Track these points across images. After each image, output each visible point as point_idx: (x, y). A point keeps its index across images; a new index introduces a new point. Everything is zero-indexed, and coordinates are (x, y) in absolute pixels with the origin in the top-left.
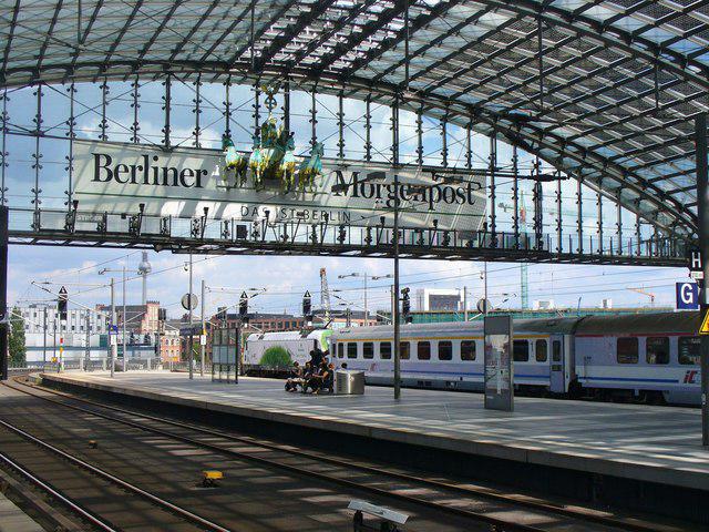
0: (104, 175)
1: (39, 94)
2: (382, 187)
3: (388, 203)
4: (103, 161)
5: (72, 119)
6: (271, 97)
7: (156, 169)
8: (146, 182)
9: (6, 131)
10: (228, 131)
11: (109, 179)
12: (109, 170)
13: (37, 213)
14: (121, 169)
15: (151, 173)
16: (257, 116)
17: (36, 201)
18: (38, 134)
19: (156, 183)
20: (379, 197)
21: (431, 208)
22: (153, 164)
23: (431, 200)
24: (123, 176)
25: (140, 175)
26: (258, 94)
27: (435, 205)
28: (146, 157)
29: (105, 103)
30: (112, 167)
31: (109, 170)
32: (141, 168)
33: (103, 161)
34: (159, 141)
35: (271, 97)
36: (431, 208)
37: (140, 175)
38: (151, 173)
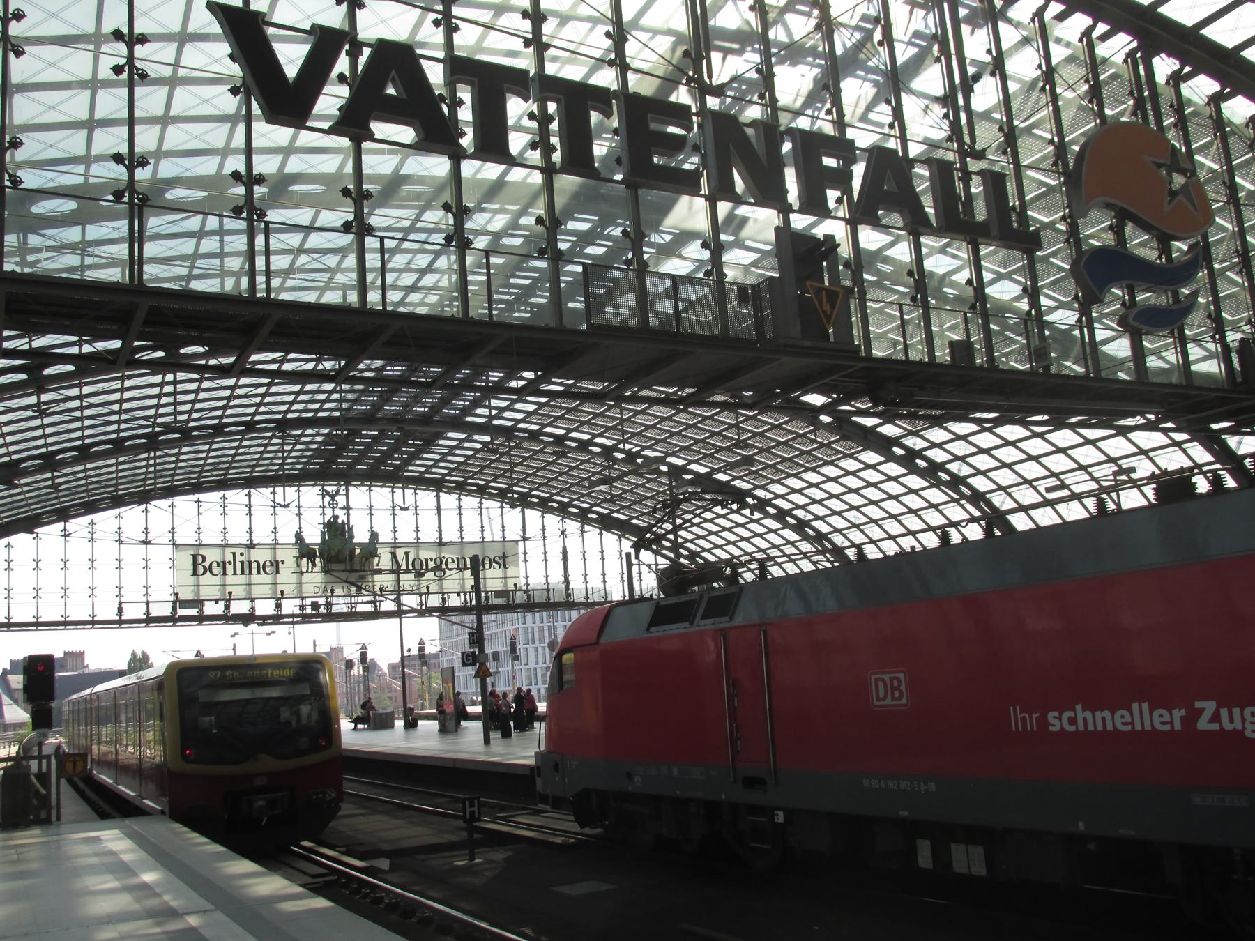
1: (146, 511)
4: (200, 559)
5: (173, 529)
6: (333, 500)
7: (242, 563)
8: (235, 573)
9: (121, 543)
10: (300, 528)
11: (205, 572)
12: (204, 567)
13: (148, 603)
14: (215, 564)
15: (239, 566)
16: (324, 514)
17: (147, 594)
18: (146, 542)
19: (243, 573)
22: (239, 558)
24: (215, 570)
25: (229, 568)
26: (323, 497)
28: (234, 554)
29: (199, 514)
30: (207, 564)
31: (204, 567)
32: (230, 563)
33: (200, 559)
34: (244, 540)
35: (333, 500)
38: (239, 566)
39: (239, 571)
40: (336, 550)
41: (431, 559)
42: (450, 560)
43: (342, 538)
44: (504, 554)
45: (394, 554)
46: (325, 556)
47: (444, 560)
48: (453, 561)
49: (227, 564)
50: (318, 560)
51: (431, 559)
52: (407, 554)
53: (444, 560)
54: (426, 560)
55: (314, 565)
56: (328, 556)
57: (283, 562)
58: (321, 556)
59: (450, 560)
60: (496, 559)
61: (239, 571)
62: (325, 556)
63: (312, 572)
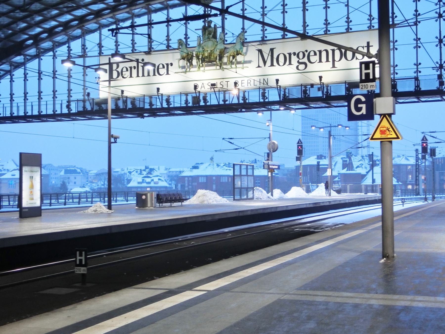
0: (115, 74)
2: (292, 56)
3: (297, 68)
12: (118, 72)
20: (290, 64)
21: (334, 66)
23: (334, 60)
25: (134, 72)
27: (336, 64)
30: (119, 70)
31: (118, 72)
32: (135, 68)
36: (334, 66)
37: (134, 72)
39: (140, 74)
40: (209, 52)
41: (294, 54)
42: (312, 53)
43: (214, 40)
44: (368, 43)
45: (260, 51)
46: (200, 57)
47: (306, 54)
48: (315, 54)
49: (133, 69)
50: (194, 62)
51: (294, 54)
52: (272, 50)
53: (306, 54)
54: (290, 54)
55: (191, 64)
56: (202, 58)
57: (172, 64)
58: (198, 57)
59: (312, 53)
60: (360, 49)
61: (140, 74)
62: (200, 57)
63: (189, 71)
